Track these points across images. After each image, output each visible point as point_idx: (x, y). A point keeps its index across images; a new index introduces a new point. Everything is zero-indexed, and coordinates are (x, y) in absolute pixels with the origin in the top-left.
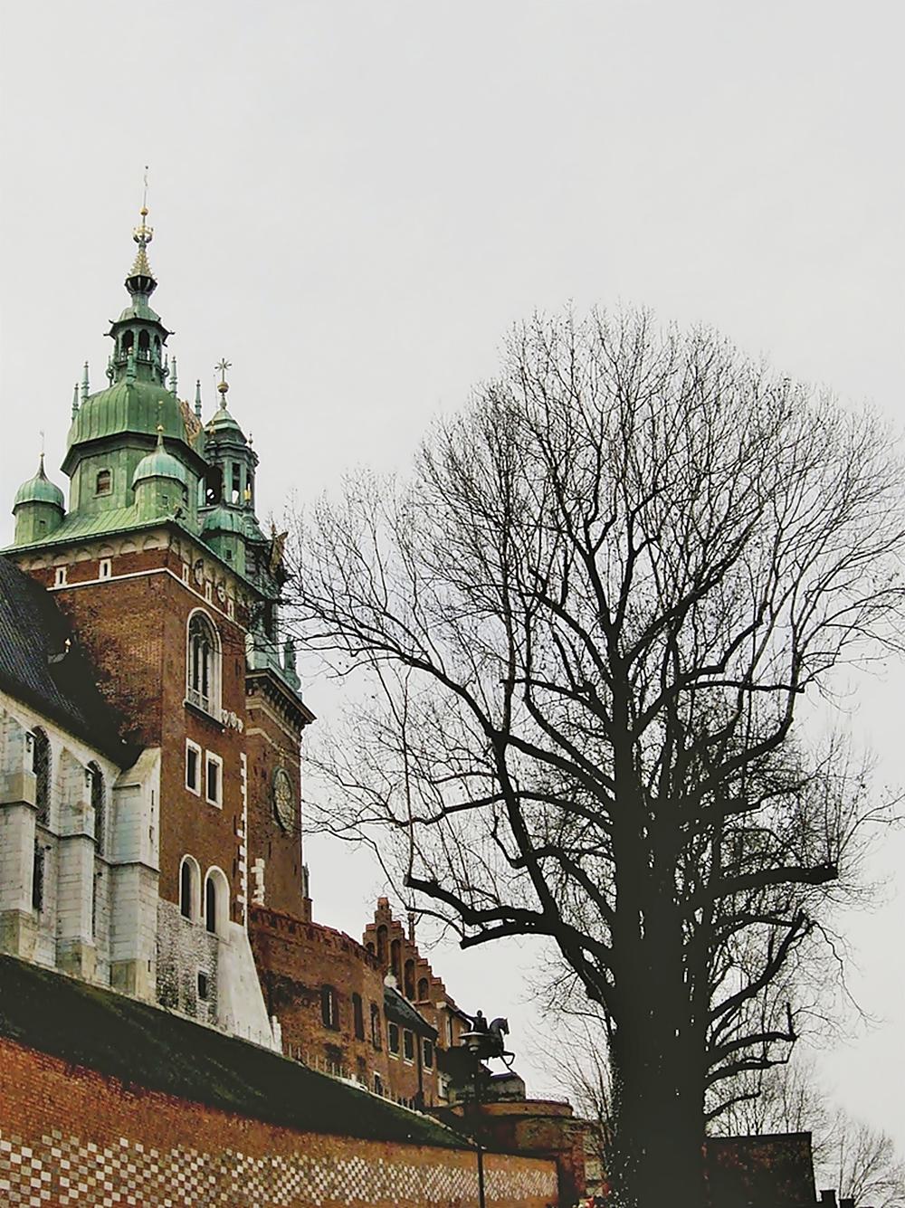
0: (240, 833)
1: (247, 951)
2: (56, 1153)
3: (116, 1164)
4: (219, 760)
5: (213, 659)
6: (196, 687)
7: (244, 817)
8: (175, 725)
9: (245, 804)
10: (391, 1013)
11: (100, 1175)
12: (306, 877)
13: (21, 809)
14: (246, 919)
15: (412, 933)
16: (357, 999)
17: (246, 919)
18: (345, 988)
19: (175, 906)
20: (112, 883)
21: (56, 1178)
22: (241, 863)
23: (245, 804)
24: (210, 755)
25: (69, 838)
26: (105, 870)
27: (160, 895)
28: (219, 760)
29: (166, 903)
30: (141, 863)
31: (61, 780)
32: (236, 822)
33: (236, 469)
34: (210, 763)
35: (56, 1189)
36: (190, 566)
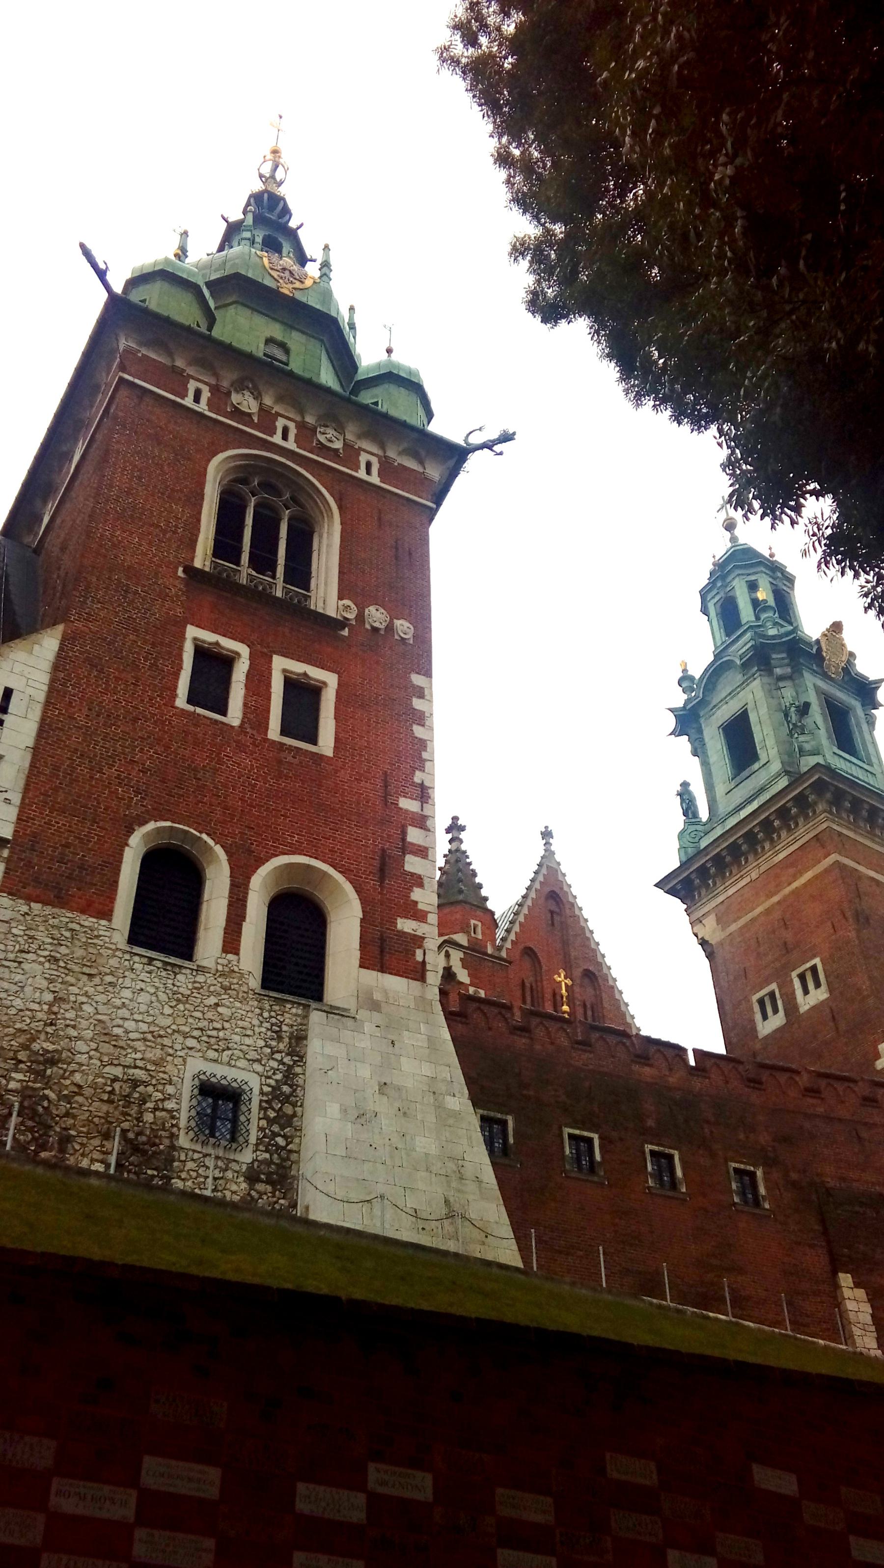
19: (89, 921)
22: (409, 858)
24: (280, 664)
33: (753, 587)
36: (215, 390)
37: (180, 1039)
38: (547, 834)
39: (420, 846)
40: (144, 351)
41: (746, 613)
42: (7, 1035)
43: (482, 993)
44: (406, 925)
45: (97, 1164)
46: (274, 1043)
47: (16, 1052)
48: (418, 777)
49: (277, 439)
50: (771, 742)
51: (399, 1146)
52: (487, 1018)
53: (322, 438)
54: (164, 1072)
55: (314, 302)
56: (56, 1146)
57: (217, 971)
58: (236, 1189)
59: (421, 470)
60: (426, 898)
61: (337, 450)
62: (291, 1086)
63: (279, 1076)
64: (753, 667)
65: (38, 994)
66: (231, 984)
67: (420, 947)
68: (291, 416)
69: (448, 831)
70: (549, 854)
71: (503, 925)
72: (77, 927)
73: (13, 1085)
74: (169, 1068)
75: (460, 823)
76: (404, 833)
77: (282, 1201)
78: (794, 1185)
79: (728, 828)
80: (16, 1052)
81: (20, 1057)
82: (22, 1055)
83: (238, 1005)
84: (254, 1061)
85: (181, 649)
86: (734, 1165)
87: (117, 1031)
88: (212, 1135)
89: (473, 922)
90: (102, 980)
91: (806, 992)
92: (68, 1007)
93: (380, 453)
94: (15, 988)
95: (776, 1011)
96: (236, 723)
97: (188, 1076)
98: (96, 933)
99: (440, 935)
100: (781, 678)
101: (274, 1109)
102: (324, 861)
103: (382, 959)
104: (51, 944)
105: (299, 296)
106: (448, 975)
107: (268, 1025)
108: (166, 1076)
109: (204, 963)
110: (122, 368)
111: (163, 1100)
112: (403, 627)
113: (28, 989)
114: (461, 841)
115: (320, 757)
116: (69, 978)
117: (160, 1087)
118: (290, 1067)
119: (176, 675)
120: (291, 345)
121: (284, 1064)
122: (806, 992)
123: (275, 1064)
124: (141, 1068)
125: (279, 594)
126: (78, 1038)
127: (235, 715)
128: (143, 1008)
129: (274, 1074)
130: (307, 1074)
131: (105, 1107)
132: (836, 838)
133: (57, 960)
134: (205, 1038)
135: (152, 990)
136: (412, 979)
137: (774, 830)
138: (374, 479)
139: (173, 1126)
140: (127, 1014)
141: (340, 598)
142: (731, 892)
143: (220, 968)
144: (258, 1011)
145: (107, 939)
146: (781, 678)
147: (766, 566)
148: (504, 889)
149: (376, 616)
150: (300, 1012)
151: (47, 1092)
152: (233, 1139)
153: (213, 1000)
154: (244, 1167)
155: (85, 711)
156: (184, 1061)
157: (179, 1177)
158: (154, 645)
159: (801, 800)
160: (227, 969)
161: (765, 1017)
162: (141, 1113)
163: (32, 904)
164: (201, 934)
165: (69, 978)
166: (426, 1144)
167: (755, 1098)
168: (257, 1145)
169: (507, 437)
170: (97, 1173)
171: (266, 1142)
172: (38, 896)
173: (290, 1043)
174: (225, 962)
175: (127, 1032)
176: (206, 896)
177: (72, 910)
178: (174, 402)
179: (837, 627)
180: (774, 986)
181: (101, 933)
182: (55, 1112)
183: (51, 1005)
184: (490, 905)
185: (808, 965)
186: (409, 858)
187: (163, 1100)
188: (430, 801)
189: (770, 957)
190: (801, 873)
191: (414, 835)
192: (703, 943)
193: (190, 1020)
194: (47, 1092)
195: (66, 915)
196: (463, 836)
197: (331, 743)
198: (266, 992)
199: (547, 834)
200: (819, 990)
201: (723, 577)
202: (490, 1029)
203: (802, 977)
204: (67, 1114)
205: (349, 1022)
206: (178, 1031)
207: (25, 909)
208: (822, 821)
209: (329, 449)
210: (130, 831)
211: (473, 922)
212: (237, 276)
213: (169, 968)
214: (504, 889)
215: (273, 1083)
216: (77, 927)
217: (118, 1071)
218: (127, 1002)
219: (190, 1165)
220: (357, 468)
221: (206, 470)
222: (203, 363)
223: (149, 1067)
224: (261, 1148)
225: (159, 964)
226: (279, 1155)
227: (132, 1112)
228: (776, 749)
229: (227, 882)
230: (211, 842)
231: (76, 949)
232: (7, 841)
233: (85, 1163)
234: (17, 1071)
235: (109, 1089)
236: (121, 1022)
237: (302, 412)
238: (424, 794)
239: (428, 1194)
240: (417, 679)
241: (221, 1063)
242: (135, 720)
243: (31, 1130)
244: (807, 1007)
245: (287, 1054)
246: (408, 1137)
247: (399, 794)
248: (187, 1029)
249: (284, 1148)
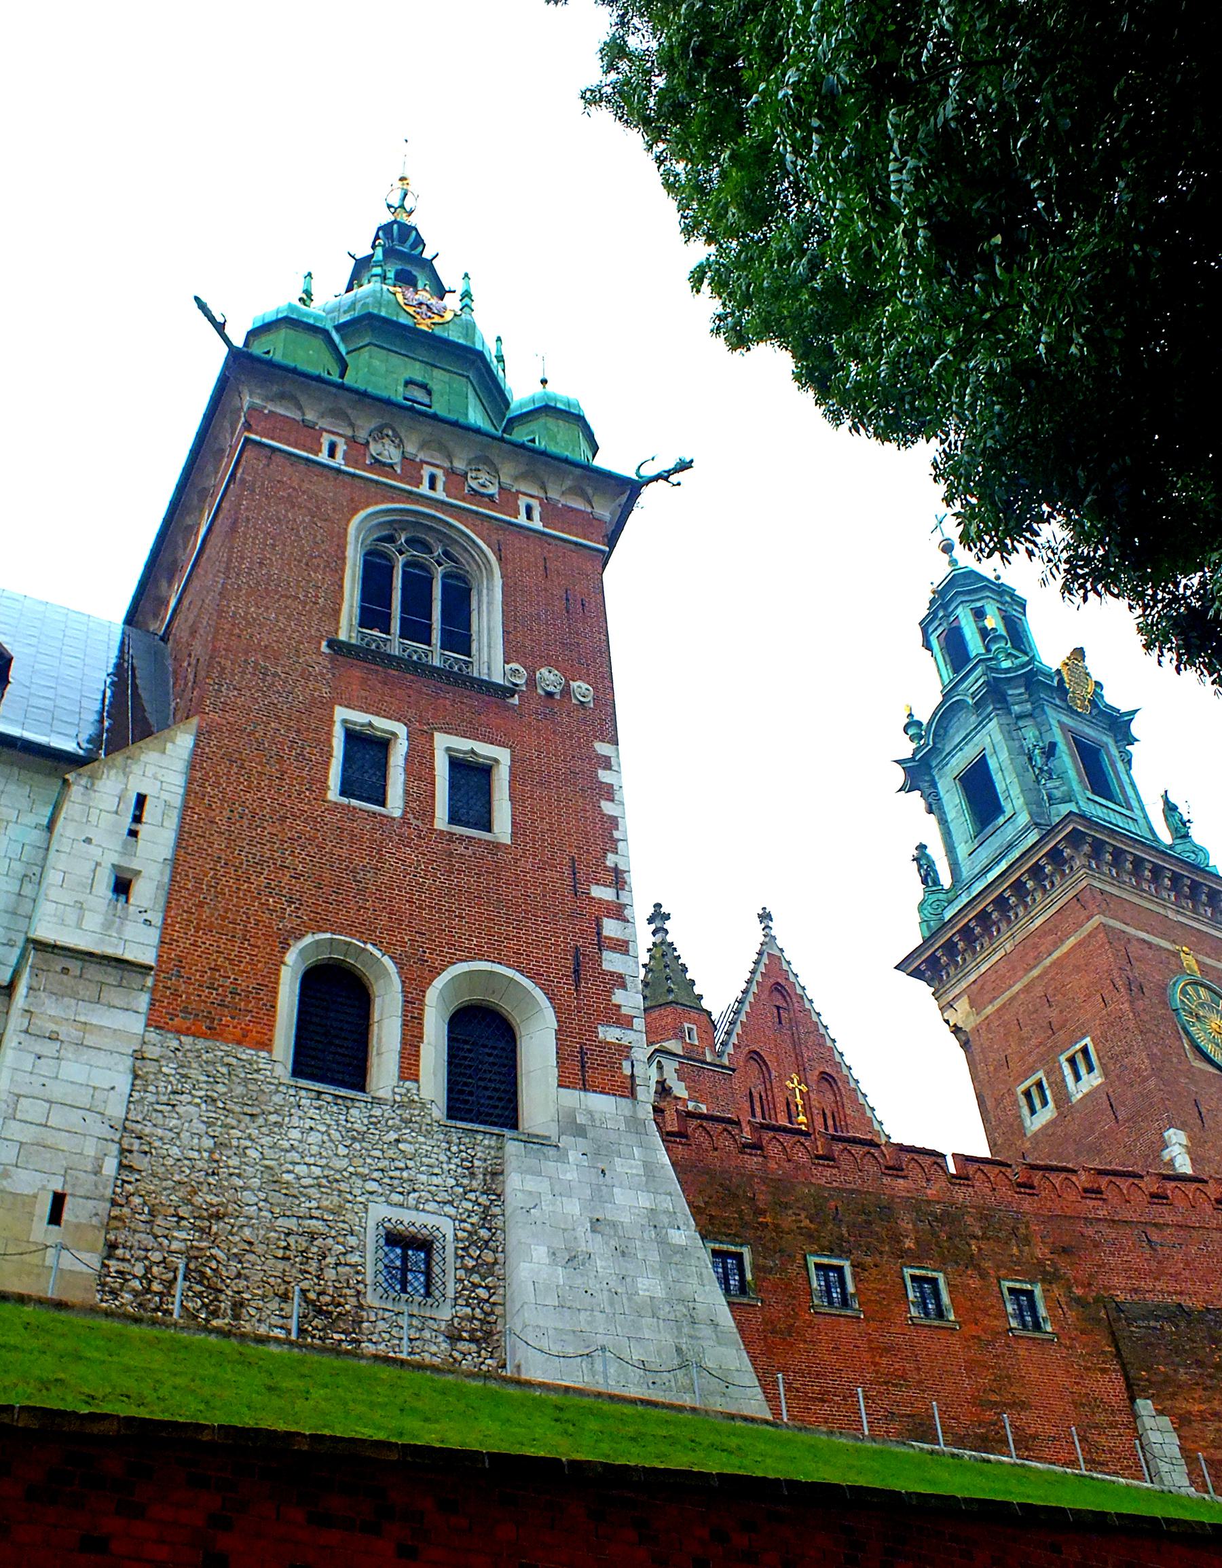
19: (247, 1054)
22: (607, 955)
24: (443, 742)
33: (979, 614)
36: (352, 441)
37: (359, 1183)
38: (765, 916)
39: (618, 940)
40: (270, 407)
41: (975, 645)
42: (165, 1189)
43: (704, 1109)
44: (610, 1034)
45: (277, 1331)
46: (466, 1181)
47: (176, 1208)
48: (611, 860)
49: (424, 489)
50: (1015, 791)
51: (619, 1291)
52: (711, 1136)
53: (474, 484)
54: (344, 1222)
55: (455, 336)
56: (229, 1312)
57: (395, 1101)
58: (436, 1350)
59: (589, 510)
60: (630, 1000)
61: (491, 496)
62: (489, 1229)
63: (475, 1219)
64: (988, 706)
65: (196, 1141)
66: (413, 1115)
67: (627, 1058)
68: (438, 462)
69: (650, 921)
70: (769, 939)
71: (723, 1027)
72: (234, 1061)
73: (175, 1246)
74: (349, 1216)
75: (663, 910)
76: (599, 926)
77: (489, 1361)
78: (1079, 1301)
79: (974, 894)
80: (176, 1208)
81: (181, 1214)
82: (183, 1211)
83: (421, 1139)
84: (445, 1203)
85: (329, 734)
86: (1007, 1284)
87: (286, 1177)
88: (404, 1290)
89: (686, 1025)
90: (266, 1120)
91: (1078, 1078)
92: (230, 1153)
93: (542, 495)
94: (171, 1135)
95: (1045, 1103)
96: (397, 813)
97: (371, 1224)
98: (255, 1067)
99: (650, 1044)
100: (1019, 717)
101: (472, 1257)
102: (509, 966)
103: (583, 1076)
104: (206, 1082)
105: (438, 331)
106: (663, 1090)
107: (458, 1161)
108: (346, 1226)
109: (380, 1094)
110: (248, 427)
111: (344, 1254)
112: (580, 687)
113: (185, 1135)
114: (666, 932)
115: (497, 846)
116: (229, 1120)
117: (341, 1239)
118: (487, 1208)
119: (327, 764)
120: (431, 385)
121: (479, 1204)
122: (1078, 1078)
123: (469, 1205)
124: (317, 1218)
125: (437, 662)
126: (244, 1188)
128: (315, 1150)
129: (469, 1216)
130: (507, 1214)
131: (281, 1265)
132: (1099, 897)
133: (214, 1100)
134: (386, 1180)
135: (324, 1129)
136: (621, 1096)
137: (1028, 893)
138: (537, 524)
139: (358, 1282)
140: (294, 1156)
141: (506, 662)
142: (983, 969)
143: (398, 1098)
144: (444, 1145)
145: (268, 1073)
146: (1019, 717)
147: (993, 591)
148: (720, 985)
149: (549, 678)
150: (493, 1143)
151: (213, 1251)
152: (428, 1294)
153: (393, 1136)
154: (443, 1326)
155: (226, 813)
156: (366, 1206)
157: (370, 1341)
158: (298, 731)
159: (1055, 856)
160: (406, 1099)
161: (1033, 1111)
162: (321, 1269)
163: (183, 1038)
164: (374, 1060)
165: (229, 1120)
166: (649, 1286)
167: (1027, 1205)
168: (456, 1299)
169: (684, 466)
170: (277, 1340)
171: (465, 1295)
172: (189, 1029)
173: (485, 1180)
174: (403, 1091)
175: (298, 1178)
176: (376, 1016)
177: (226, 1041)
178: (307, 459)
179: (1079, 653)
180: (1040, 1074)
181: (261, 1066)
182: (224, 1273)
183: (211, 1152)
184: (705, 1004)
185: (1078, 1047)
186: (607, 955)
187: (344, 1254)
188: (627, 888)
189: (1034, 1042)
190: (1062, 941)
191: (611, 928)
192: (956, 1030)
193: (369, 1161)
194: (213, 1251)
195: (221, 1048)
196: (668, 925)
197: (508, 829)
198: (453, 1123)
199: (765, 916)
200: (1092, 1075)
201: (944, 606)
202: (716, 1149)
203: (1072, 1061)
204: (239, 1276)
205: (552, 1152)
206: (356, 1174)
207: (175, 1044)
208: (1082, 876)
209: (483, 495)
210: (285, 947)
211: (686, 1025)
212: (370, 316)
213: (340, 1101)
214: (720, 985)
215: (467, 1226)
216: (234, 1061)
217: (292, 1223)
218: (296, 1143)
219: (382, 1325)
220: (516, 514)
221: (346, 530)
222: (337, 414)
223: (326, 1217)
224: (460, 1301)
225: (329, 1098)
226: (482, 1309)
227: (310, 1270)
228: (1022, 800)
229: (400, 997)
230: (378, 954)
231: (233, 1086)
232: (151, 968)
233: (263, 1330)
234: (178, 1228)
235: (284, 1244)
236: (291, 1167)
237: (450, 458)
238: (618, 879)
239: (656, 1342)
240: (602, 748)
241: (408, 1208)
242: (283, 819)
243: (199, 1295)
244: (1079, 1096)
245: (483, 1193)
246: (628, 1280)
247: (589, 882)
248: (366, 1171)
249: (487, 1301)
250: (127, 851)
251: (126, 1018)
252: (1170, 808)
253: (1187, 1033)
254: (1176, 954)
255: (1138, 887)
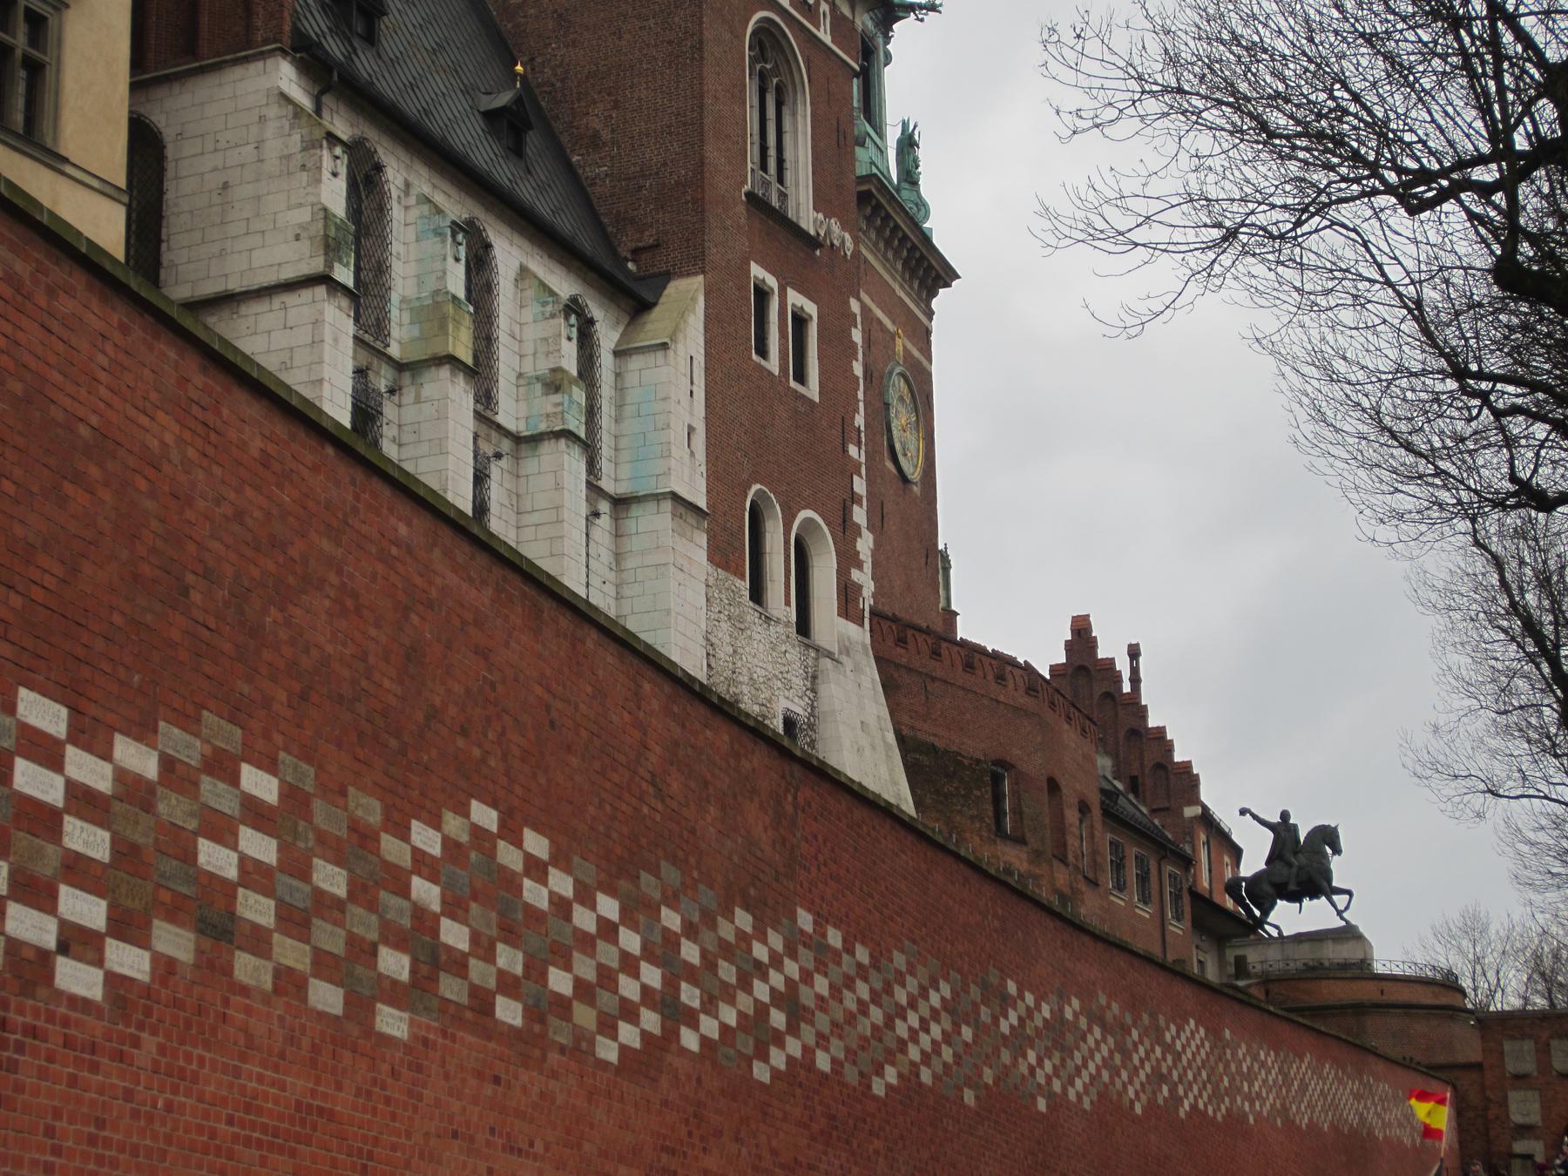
0: (853, 450)
1: (871, 673)
2: (671, 920)
3: (792, 969)
4: (811, 308)
5: (794, 114)
6: (764, 167)
7: (860, 420)
8: (728, 227)
9: (860, 395)
10: (1112, 816)
11: (761, 991)
12: (947, 569)
13: (445, 372)
14: (867, 614)
15: (1135, 680)
16: (1053, 786)
17: (867, 614)
18: (1034, 765)
19: (738, 582)
20: (618, 535)
21: (671, 983)
22: (856, 508)
23: (860, 395)
24: (795, 298)
25: (536, 439)
26: (604, 507)
27: (711, 559)
28: (811, 308)
29: (722, 573)
30: (675, 497)
31: (517, 329)
32: (846, 432)
34: (794, 315)
35: (677, 1015)
127: (773, 364)
138: (827, 39)
250: (692, 414)
251: (696, 549)
252: (908, 144)
253: (889, 430)
254: (893, 337)
255: (876, 245)
